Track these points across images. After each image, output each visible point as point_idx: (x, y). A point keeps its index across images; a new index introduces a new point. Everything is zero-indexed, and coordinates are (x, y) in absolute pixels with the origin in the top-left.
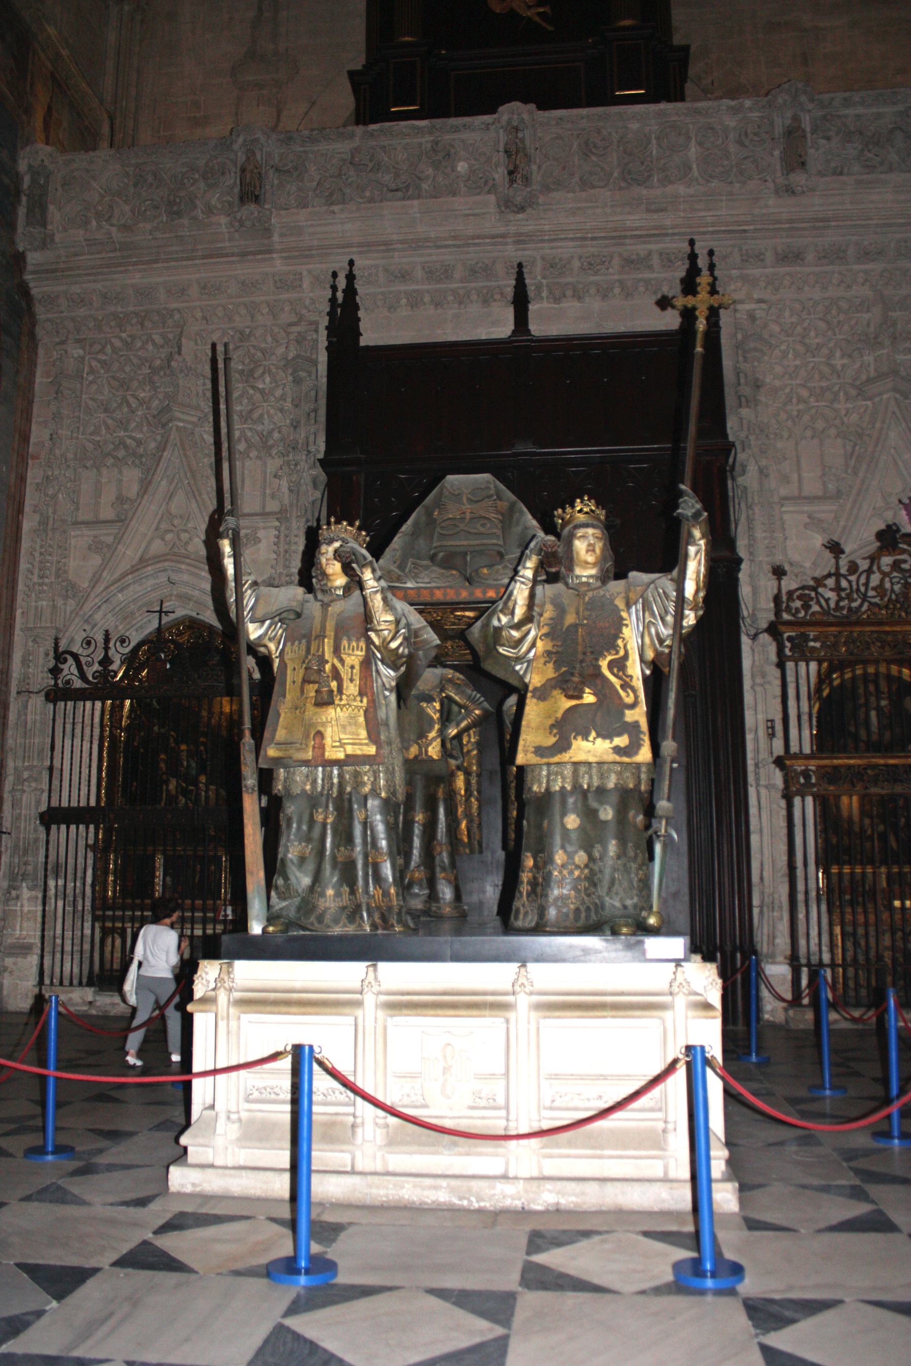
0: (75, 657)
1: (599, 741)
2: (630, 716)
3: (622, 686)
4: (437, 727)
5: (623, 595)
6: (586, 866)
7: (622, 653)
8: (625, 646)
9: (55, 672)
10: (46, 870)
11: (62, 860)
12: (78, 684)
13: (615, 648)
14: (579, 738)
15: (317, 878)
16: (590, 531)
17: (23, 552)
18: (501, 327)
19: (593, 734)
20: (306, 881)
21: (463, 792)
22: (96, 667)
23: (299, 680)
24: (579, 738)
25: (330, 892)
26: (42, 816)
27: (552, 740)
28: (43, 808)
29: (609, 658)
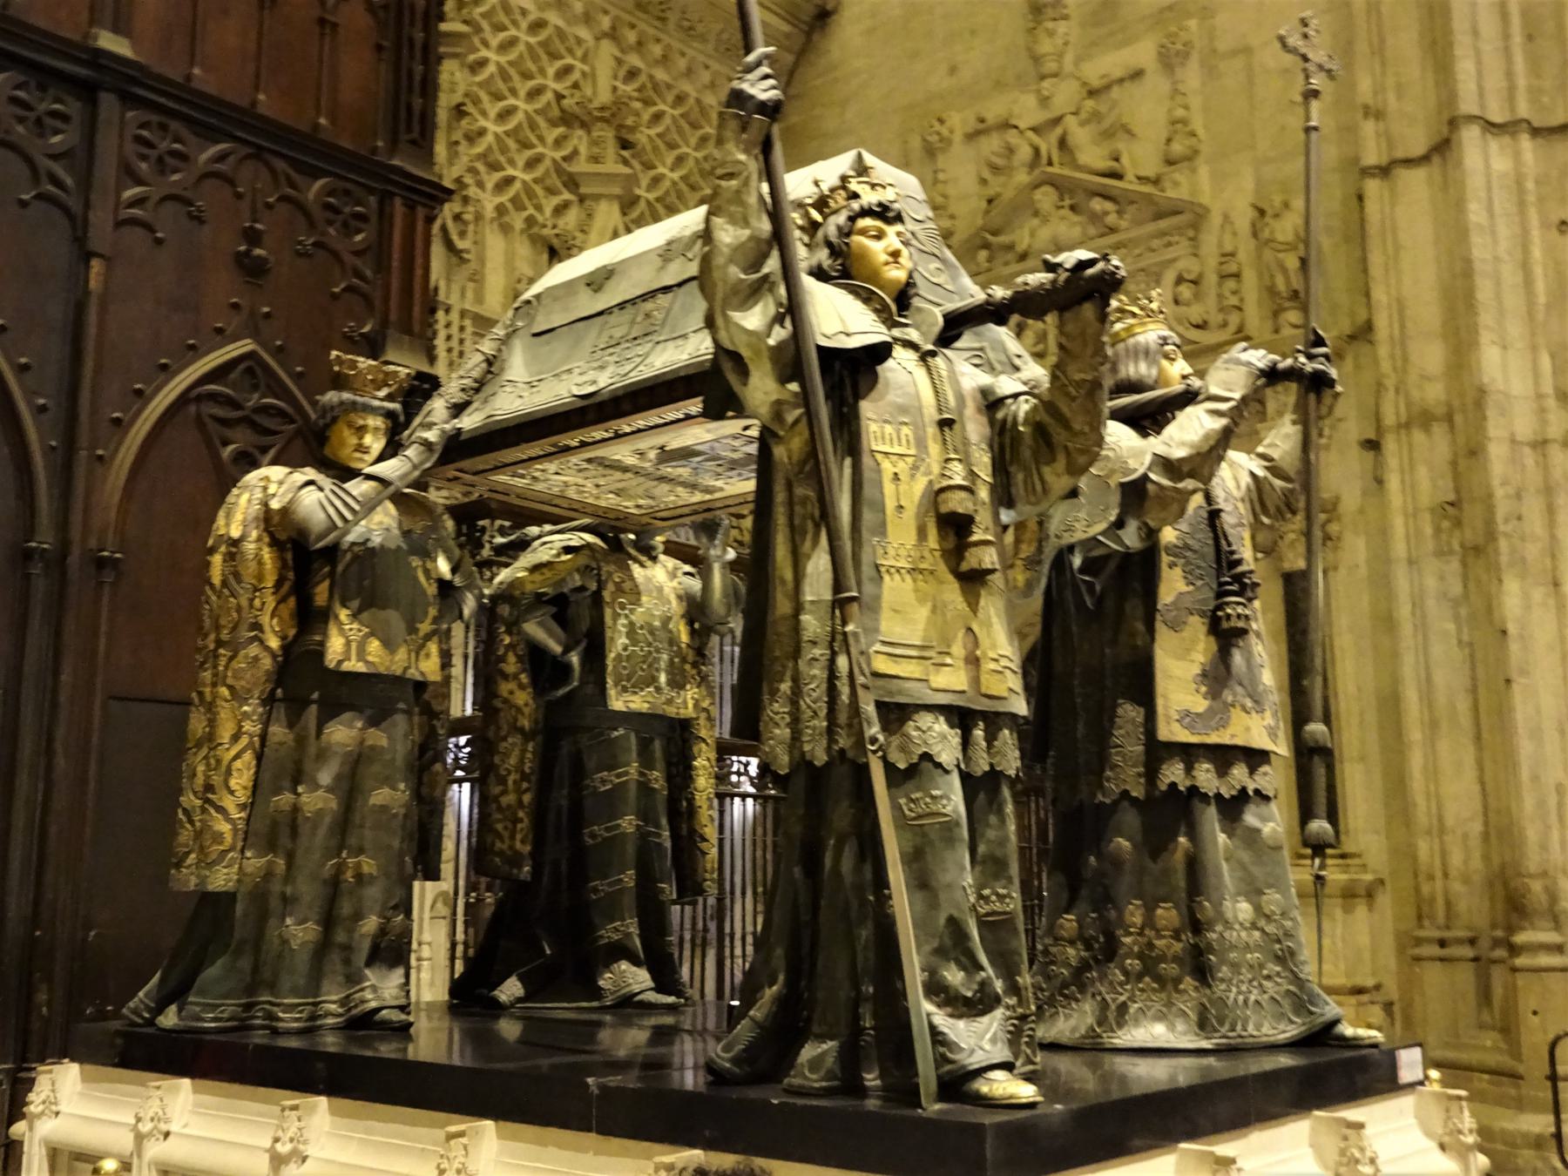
4: (433, 612)
6: (1254, 926)
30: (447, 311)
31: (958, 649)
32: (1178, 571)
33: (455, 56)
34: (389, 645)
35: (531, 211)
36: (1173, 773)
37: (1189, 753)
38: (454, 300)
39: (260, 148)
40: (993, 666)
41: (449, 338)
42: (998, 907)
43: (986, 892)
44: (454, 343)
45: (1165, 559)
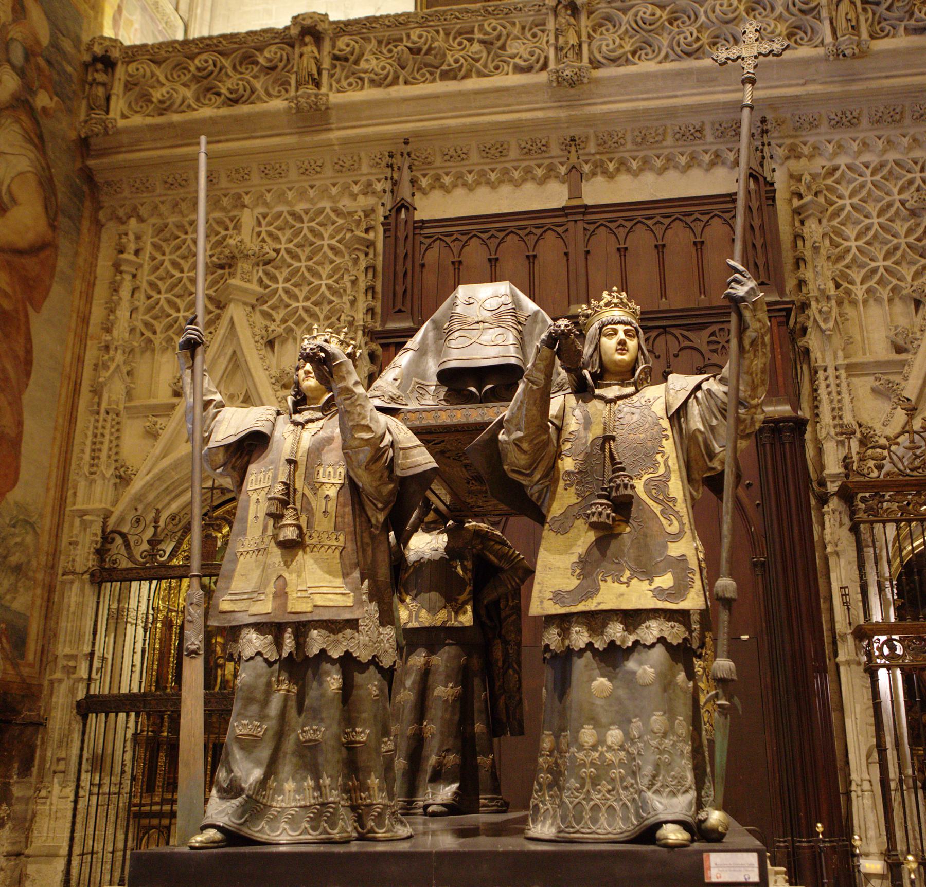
0: (124, 536)
1: (634, 582)
2: (675, 550)
3: (662, 512)
5: (663, 400)
7: (662, 470)
8: (666, 461)
9: (101, 553)
10: (80, 764)
11: (109, 751)
12: (125, 564)
13: (655, 465)
14: (609, 579)
15: (271, 769)
16: (621, 328)
17: (77, 431)
18: (555, 196)
19: (628, 573)
20: (257, 774)
21: (500, 664)
22: (145, 546)
23: (262, 515)
24: (609, 579)
25: (290, 785)
26: (79, 704)
27: (574, 583)
28: (81, 695)
29: (646, 477)
30: (825, 370)
31: (271, 589)
32: (572, 490)
33: (809, 216)
34: (432, 610)
35: (895, 282)
36: (552, 638)
37: (563, 622)
38: (830, 363)
39: (664, 327)
40: (299, 594)
41: (828, 386)
42: (313, 737)
43: (306, 728)
44: (833, 388)
45: (561, 483)
